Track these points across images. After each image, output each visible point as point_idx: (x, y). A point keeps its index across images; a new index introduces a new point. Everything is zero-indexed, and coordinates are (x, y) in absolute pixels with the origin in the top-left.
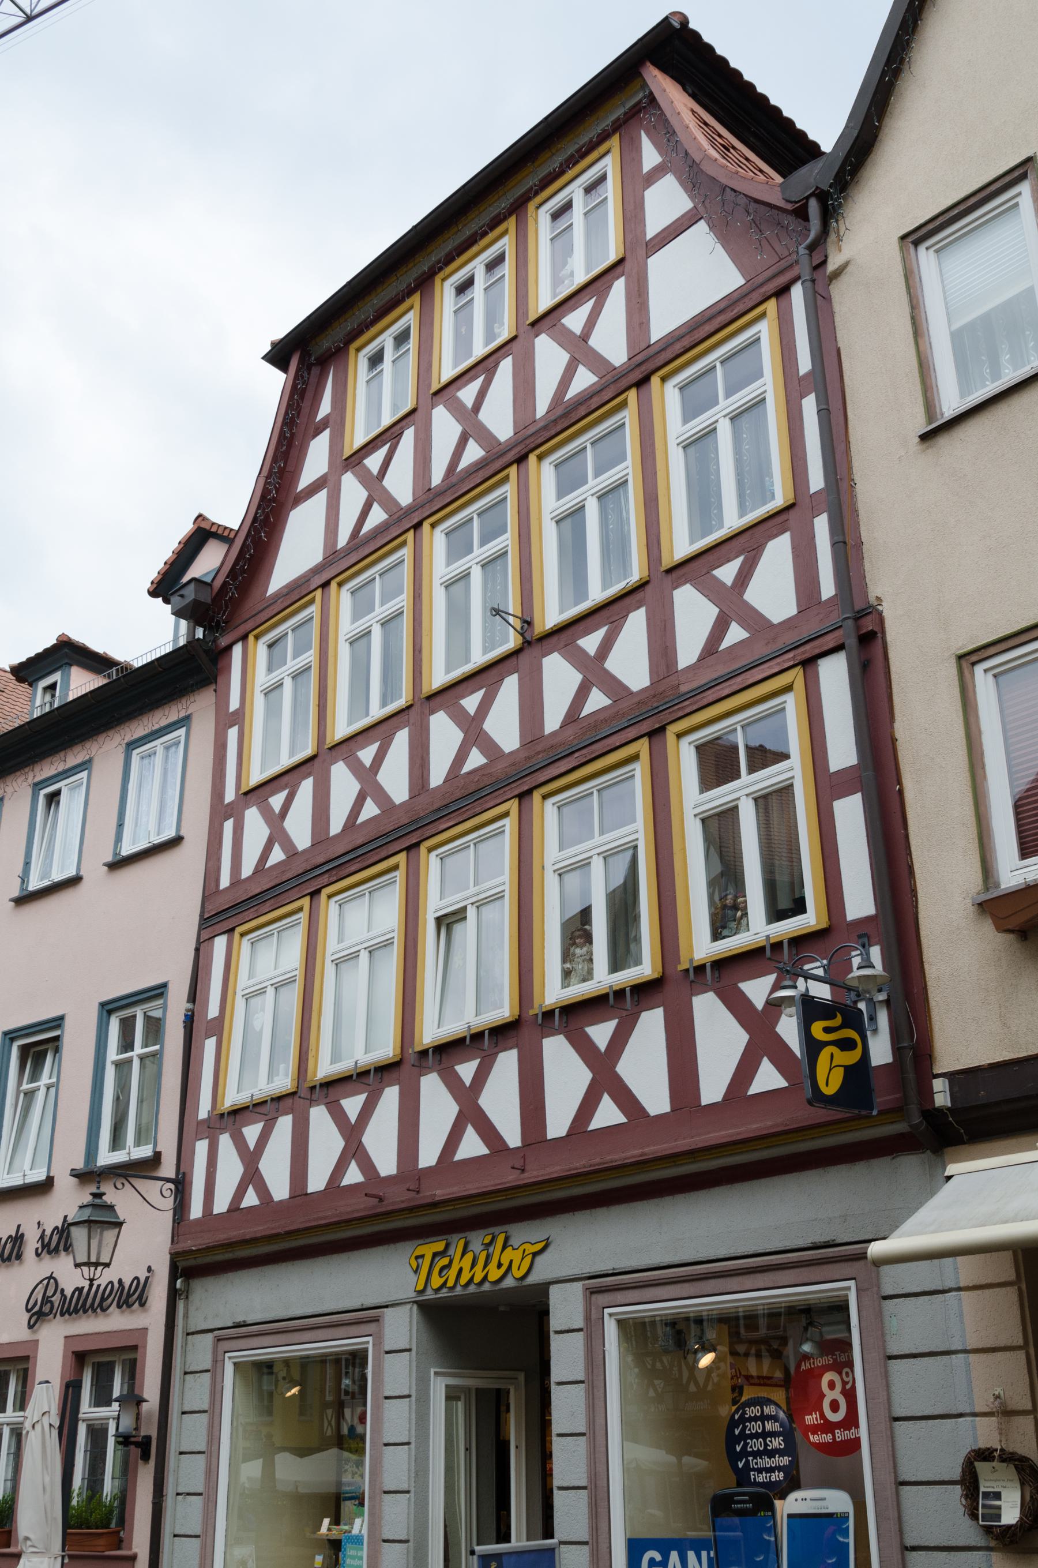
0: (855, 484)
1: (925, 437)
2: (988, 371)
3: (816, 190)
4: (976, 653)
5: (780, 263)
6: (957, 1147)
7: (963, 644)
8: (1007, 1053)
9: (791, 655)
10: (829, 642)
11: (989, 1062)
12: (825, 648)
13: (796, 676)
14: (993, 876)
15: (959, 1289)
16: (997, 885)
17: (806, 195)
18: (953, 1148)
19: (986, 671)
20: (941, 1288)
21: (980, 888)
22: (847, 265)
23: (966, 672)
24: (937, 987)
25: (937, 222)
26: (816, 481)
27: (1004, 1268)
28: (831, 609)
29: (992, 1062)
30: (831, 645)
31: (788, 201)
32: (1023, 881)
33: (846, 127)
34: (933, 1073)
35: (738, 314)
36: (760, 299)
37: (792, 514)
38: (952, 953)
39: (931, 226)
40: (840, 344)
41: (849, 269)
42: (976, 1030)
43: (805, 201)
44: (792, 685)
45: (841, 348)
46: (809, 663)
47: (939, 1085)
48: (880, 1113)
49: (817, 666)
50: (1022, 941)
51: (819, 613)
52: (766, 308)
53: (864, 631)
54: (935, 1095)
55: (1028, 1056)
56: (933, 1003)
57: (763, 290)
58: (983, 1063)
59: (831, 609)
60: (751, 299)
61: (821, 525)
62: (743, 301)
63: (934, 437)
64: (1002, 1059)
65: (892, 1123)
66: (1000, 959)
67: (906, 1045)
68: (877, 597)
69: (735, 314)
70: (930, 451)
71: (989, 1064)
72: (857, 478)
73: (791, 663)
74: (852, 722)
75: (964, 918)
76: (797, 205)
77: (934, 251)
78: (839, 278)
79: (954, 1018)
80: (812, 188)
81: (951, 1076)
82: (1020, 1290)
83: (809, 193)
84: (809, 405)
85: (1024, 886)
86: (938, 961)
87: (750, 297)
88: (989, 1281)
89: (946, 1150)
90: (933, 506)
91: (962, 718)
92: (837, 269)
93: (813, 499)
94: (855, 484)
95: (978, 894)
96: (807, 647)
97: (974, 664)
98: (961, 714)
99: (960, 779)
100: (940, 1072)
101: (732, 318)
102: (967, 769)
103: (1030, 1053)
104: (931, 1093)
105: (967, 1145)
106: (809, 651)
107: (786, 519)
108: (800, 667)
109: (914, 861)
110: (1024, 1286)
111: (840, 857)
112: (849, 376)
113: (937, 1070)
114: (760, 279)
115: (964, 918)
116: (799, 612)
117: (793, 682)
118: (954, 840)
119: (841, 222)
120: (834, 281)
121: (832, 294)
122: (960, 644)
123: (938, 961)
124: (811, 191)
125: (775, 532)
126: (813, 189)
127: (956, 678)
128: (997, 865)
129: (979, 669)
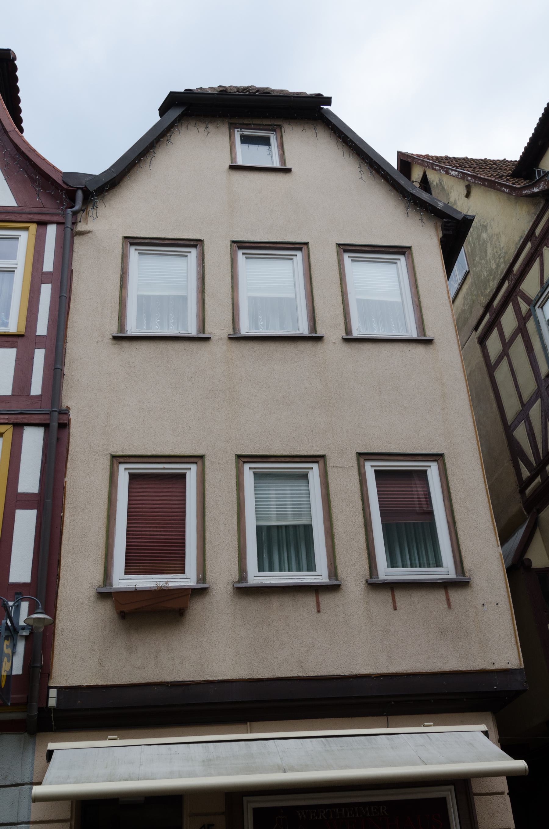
0: (67, 342)
1: (115, 338)
2: (145, 322)
3: (84, 188)
4: (123, 458)
5: (42, 209)
6: (46, 733)
7: (116, 450)
8: (99, 681)
9: (7, 417)
10: (36, 419)
11: (86, 684)
12: (32, 422)
13: (8, 430)
14: (110, 580)
15: (28, 823)
16: (111, 585)
17: (78, 187)
18: (44, 733)
19: (126, 469)
20: (16, 822)
21: (100, 584)
22: (89, 233)
23: (115, 465)
24: (61, 634)
25: (146, 241)
26: (42, 329)
27: (64, 811)
28: (36, 401)
29: (89, 684)
30: (37, 421)
31: (64, 182)
32: (134, 586)
33: (109, 169)
34: (48, 685)
35: (11, 220)
36: (27, 220)
37: (20, 340)
38: (76, 617)
39: (142, 241)
40: (73, 268)
41: (89, 235)
42: (82, 664)
43: (76, 189)
44: (3, 434)
45: (74, 271)
46: (19, 426)
47: (53, 693)
48: (12, 705)
49: (23, 429)
50: (122, 619)
51: (27, 400)
52: (29, 226)
53: (61, 422)
54: (49, 699)
55: (113, 685)
56: (56, 644)
57: (31, 216)
58: (83, 685)
59: (36, 401)
60: (21, 216)
61: (39, 355)
62: (16, 215)
63: (121, 340)
64: (95, 684)
65: (10, 712)
66: (105, 626)
67: (38, 665)
68: (67, 406)
69: (8, 219)
70: (117, 346)
71: (87, 686)
72: (68, 339)
73: (6, 422)
74: (40, 469)
75: (87, 598)
76: (70, 188)
77: (138, 253)
78: (81, 236)
79: (68, 655)
80: (82, 185)
81: (60, 689)
82: (71, 825)
83: (80, 187)
84: (46, 290)
85: (133, 590)
86: (65, 619)
87: (21, 215)
88: (52, 818)
89: (38, 734)
90: (112, 374)
91: (108, 488)
92: (83, 231)
93: (37, 338)
94: (67, 342)
95: (99, 587)
96: (19, 416)
97: (120, 463)
98: (107, 486)
99: (100, 521)
100: (52, 685)
101: (5, 219)
102: (105, 517)
103: (114, 683)
104: (48, 697)
105: (53, 733)
106: (20, 419)
107: (16, 341)
108: (12, 426)
109: (62, 558)
110: (73, 823)
111: (13, 543)
112: (75, 287)
113: (51, 684)
114: (28, 210)
115: (87, 598)
116: (12, 395)
117: (4, 433)
118: (90, 553)
119: (95, 212)
120: (78, 236)
121: (74, 241)
122: (115, 450)
123: (65, 619)
124: (82, 187)
125: (6, 345)
126: (83, 187)
127: (109, 467)
128: (113, 574)
129: (122, 467)
